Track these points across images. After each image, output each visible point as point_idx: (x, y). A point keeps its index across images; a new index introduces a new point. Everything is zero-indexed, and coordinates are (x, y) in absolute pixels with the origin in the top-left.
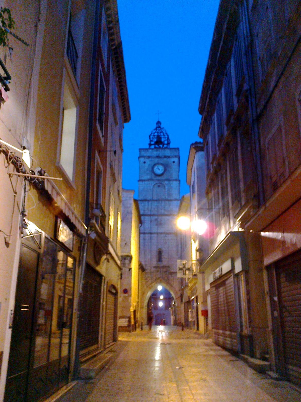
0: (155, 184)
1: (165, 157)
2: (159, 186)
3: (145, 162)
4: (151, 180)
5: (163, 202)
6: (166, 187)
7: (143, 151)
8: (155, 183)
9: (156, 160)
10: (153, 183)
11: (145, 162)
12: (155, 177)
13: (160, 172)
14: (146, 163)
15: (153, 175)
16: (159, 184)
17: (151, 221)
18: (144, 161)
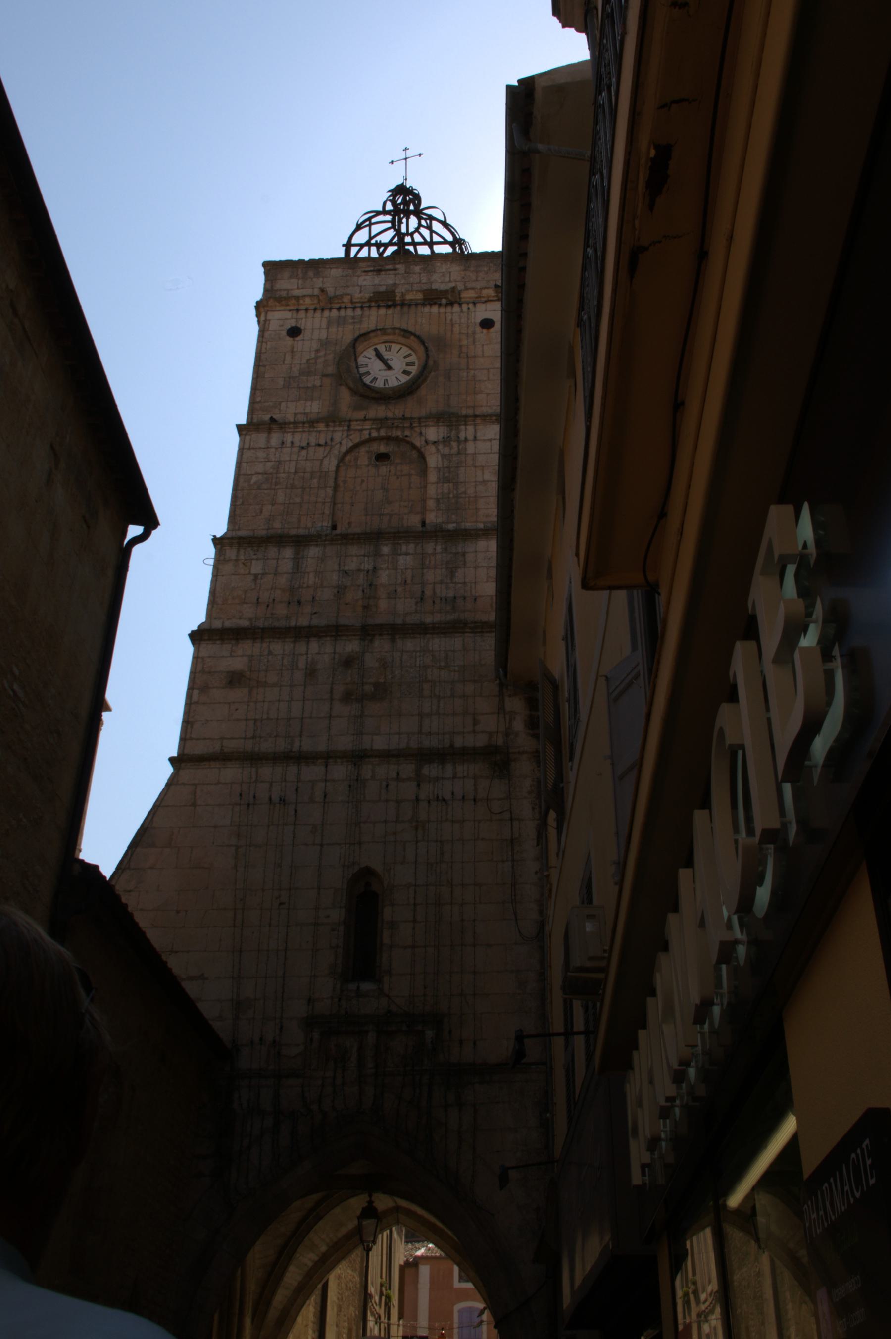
0: (356, 446)
2: (382, 457)
3: (294, 332)
6: (433, 460)
7: (291, 277)
8: (356, 438)
9: (374, 318)
10: (342, 440)
11: (294, 332)
13: (395, 378)
14: (306, 335)
15: (346, 396)
16: (383, 449)
17: (311, 673)
18: (291, 323)
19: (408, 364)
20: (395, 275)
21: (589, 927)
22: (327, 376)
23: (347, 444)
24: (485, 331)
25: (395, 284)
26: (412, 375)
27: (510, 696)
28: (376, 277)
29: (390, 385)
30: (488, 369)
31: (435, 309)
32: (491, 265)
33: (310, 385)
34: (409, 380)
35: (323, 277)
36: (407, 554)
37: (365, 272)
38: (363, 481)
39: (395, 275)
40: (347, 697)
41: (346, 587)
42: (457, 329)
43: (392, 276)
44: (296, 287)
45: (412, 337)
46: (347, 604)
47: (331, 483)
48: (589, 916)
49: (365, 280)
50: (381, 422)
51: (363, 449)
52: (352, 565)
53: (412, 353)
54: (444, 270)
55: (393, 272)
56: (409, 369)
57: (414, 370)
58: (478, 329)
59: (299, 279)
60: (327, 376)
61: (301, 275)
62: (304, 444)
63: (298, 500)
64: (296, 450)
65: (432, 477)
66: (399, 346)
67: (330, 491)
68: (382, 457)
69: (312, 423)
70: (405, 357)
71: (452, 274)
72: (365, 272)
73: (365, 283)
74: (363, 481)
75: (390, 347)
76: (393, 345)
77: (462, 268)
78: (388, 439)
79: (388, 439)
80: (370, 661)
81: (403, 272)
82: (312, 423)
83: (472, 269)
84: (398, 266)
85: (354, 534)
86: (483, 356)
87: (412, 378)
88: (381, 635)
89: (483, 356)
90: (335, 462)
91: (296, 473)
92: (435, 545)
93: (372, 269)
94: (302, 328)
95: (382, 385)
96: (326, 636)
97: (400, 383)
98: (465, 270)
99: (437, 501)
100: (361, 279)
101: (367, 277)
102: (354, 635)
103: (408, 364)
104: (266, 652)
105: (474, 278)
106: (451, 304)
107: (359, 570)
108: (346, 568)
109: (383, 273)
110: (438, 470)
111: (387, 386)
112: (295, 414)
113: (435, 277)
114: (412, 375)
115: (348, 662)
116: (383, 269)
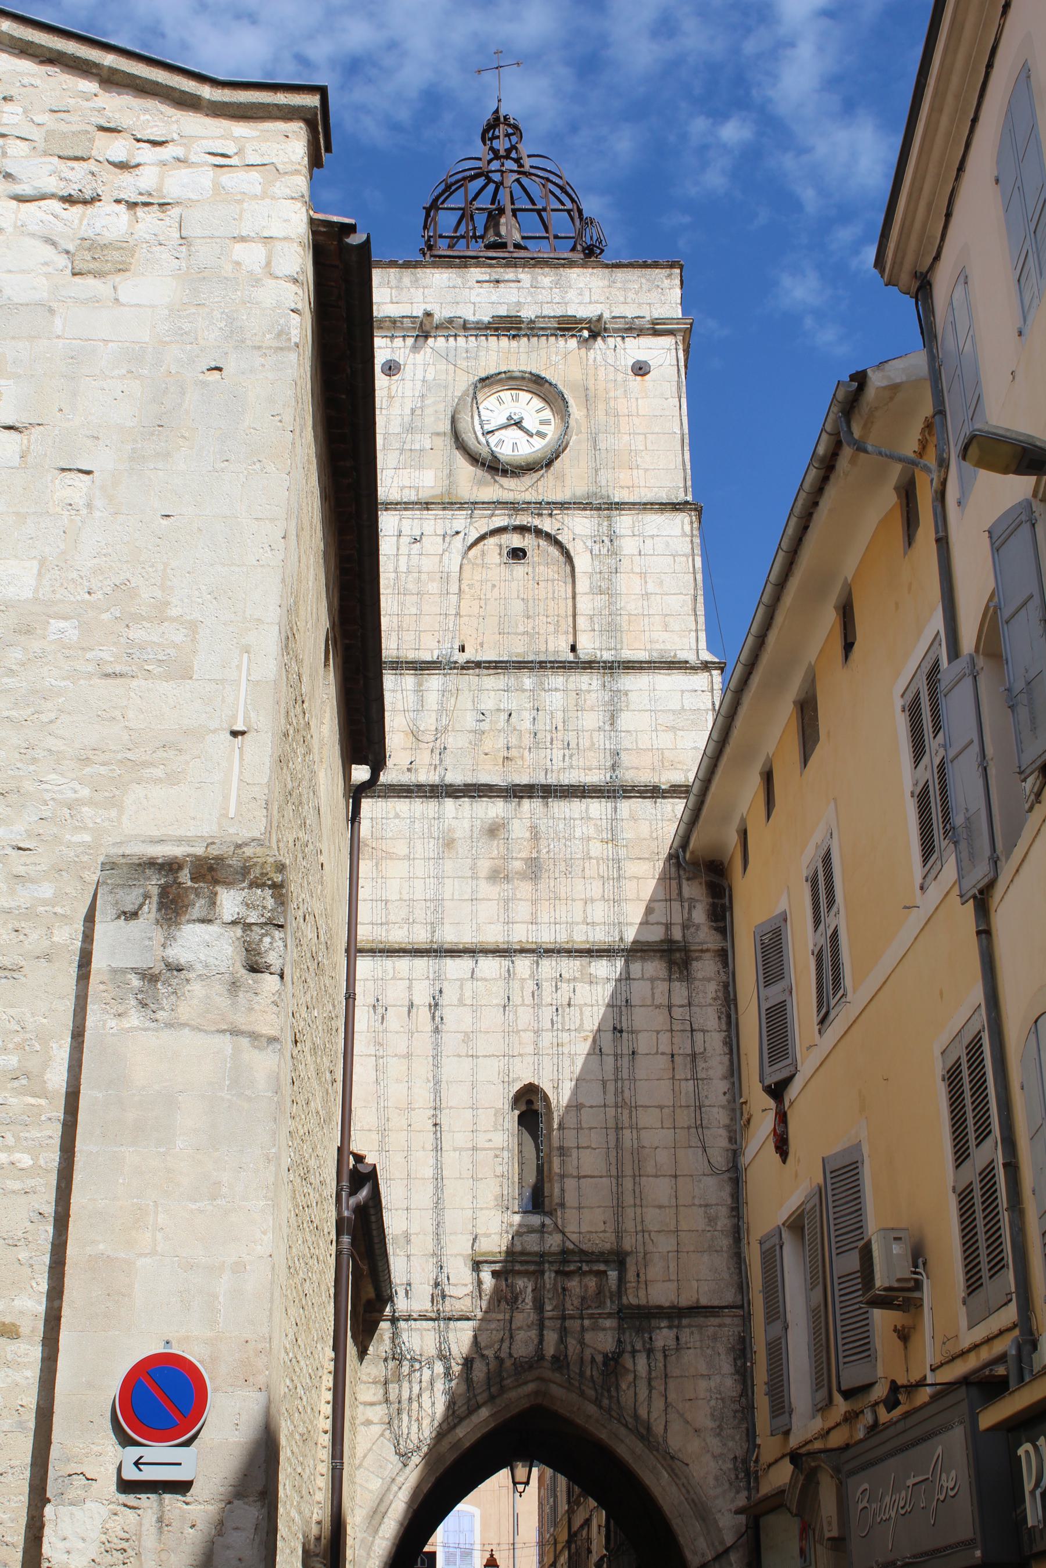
0: (482, 538)
1: (567, 326)
2: (517, 554)
4: (450, 504)
5: (557, 680)
6: (582, 562)
12: (481, 483)
14: (407, 372)
15: (465, 469)
16: (516, 541)
17: (449, 843)
19: (543, 422)
20: (519, 288)
21: (896, 1249)
22: (438, 434)
23: (474, 535)
24: (639, 378)
25: (519, 303)
26: (548, 439)
27: (688, 879)
28: (493, 290)
29: (521, 453)
30: (645, 434)
31: (573, 343)
32: (643, 281)
33: (418, 447)
34: (546, 446)
35: (424, 287)
36: (556, 690)
37: (478, 282)
38: (494, 586)
39: (519, 288)
40: (496, 876)
41: (483, 732)
42: (601, 372)
43: (515, 291)
44: (388, 300)
45: (547, 385)
46: (486, 754)
47: (454, 588)
48: (895, 1239)
49: (478, 295)
50: (514, 507)
51: (492, 541)
52: (488, 703)
53: (547, 406)
54: (581, 285)
55: (516, 284)
56: (544, 429)
57: (551, 431)
58: (631, 376)
59: (391, 288)
60: (438, 434)
61: (393, 283)
62: (417, 533)
63: (414, 611)
64: (408, 540)
65: (582, 585)
66: (529, 396)
67: (454, 599)
68: (517, 554)
69: (427, 505)
70: (538, 411)
71: (593, 291)
72: (478, 282)
73: (478, 299)
74: (494, 586)
75: (517, 396)
76: (521, 393)
77: (606, 283)
78: (522, 529)
79: (522, 529)
80: (519, 830)
81: (529, 286)
82: (427, 505)
83: (619, 285)
84: (521, 276)
85: (490, 662)
86: (638, 415)
87: (549, 443)
88: (530, 797)
89: (638, 415)
90: (457, 559)
91: (409, 572)
92: (591, 679)
93: (487, 278)
94: (401, 362)
95: (510, 452)
96: (464, 797)
97: (534, 450)
98: (609, 287)
99: (591, 618)
100: (474, 292)
101: (481, 290)
102: (498, 797)
103: (543, 422)
104: (391, 815)
105: (622, 299)
106: (594, 335)
107: (498, 710)
108: (482, 707)
109: (502, 285)
110: (591, 575)
111: (516, 453)
112: (402, 488)
113: (571, 295)
114: (548, 439)
115: (493, 830)
116: (502, 279)
